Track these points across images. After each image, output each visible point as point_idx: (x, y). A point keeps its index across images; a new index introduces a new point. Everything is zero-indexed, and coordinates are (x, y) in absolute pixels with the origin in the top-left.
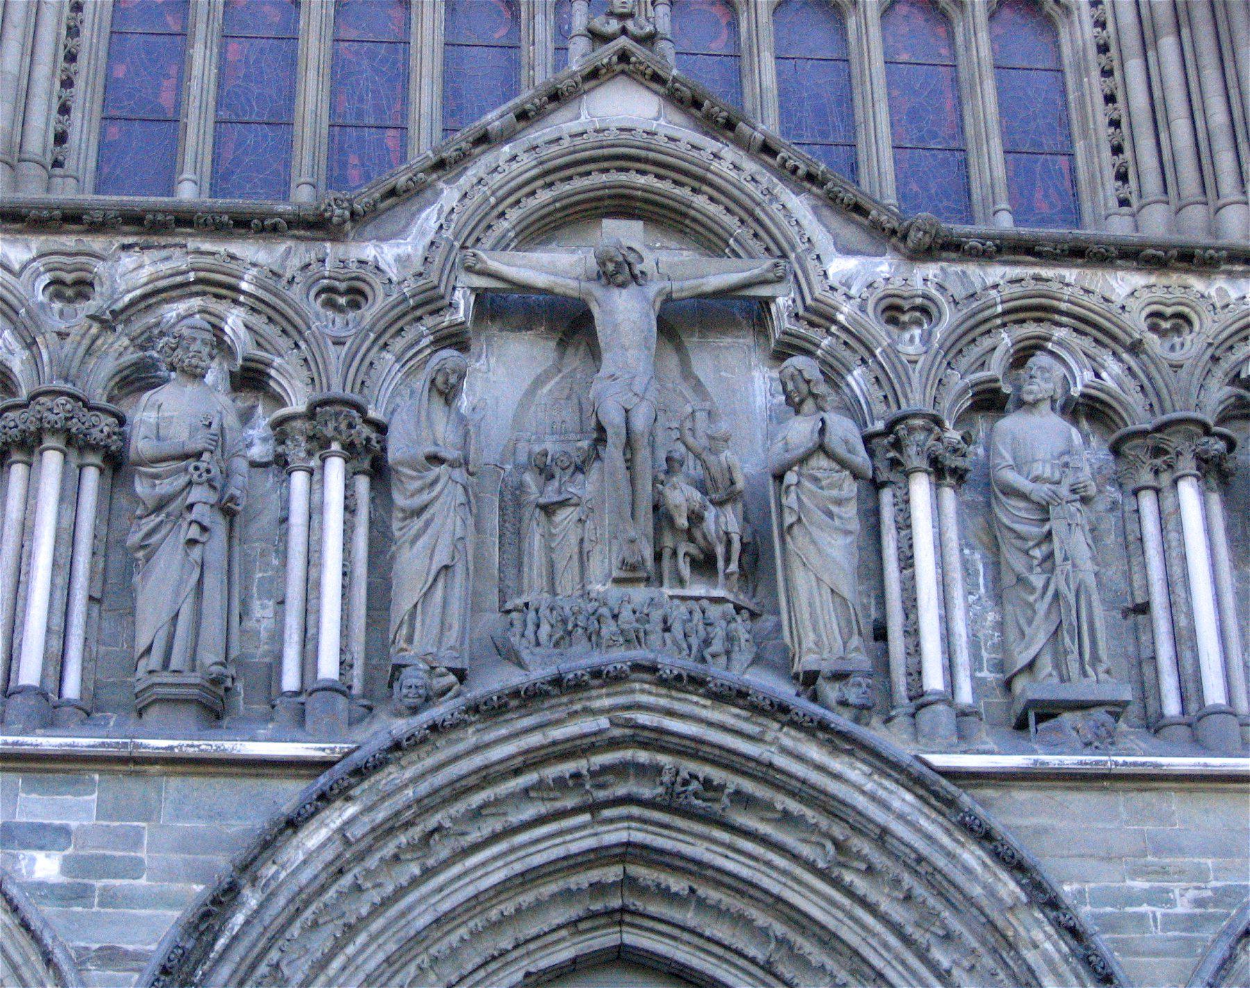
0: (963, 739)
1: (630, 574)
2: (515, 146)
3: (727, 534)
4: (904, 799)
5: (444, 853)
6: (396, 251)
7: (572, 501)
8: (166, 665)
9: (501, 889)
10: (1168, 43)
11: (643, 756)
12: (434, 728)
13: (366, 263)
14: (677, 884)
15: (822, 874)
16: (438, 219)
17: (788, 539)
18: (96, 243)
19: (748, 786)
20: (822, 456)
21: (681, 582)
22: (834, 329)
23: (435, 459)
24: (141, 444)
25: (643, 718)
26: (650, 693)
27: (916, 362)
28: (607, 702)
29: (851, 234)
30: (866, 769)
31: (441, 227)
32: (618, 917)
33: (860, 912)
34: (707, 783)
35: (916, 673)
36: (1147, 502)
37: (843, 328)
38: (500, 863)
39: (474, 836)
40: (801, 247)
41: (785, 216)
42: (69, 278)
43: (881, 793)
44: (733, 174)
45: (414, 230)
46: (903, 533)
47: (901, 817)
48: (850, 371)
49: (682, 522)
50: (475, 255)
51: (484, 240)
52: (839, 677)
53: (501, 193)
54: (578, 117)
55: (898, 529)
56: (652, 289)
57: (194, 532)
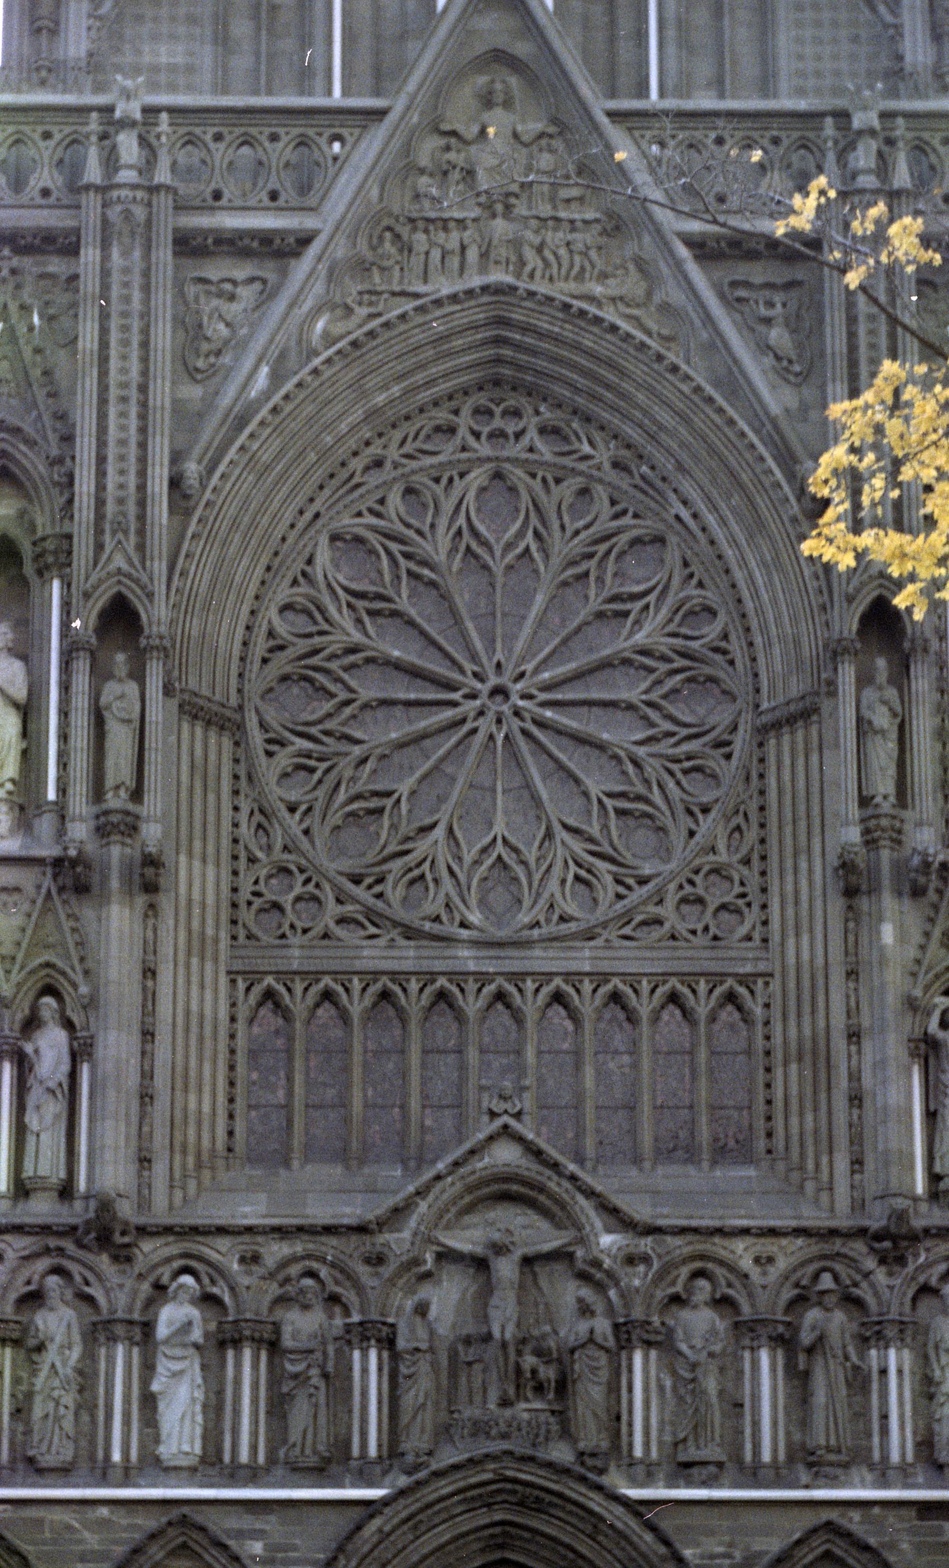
0: (649, 1480)
1: (505, 1403)
4: (619, 1510)
8: (303, 1451)
9: (448, 1543)
10: (794, 1067)
11: (509, 1486)
14: (526, 1535)
15: (589, 1536)
18: (260, 1239)
21: (527, 1400)
23: (417, 1350)
24: (287, 1342)
25: (509, 1473)
29: (612, 1221)
32: (501, 1547)
33: (605, 1553)
35: (631, 1445)
36: (747, 1355)
42: (249, 1255)
49: (528, 1375)
52: (593, 1455)
56: (518, 1253)
57: (312, 1390)
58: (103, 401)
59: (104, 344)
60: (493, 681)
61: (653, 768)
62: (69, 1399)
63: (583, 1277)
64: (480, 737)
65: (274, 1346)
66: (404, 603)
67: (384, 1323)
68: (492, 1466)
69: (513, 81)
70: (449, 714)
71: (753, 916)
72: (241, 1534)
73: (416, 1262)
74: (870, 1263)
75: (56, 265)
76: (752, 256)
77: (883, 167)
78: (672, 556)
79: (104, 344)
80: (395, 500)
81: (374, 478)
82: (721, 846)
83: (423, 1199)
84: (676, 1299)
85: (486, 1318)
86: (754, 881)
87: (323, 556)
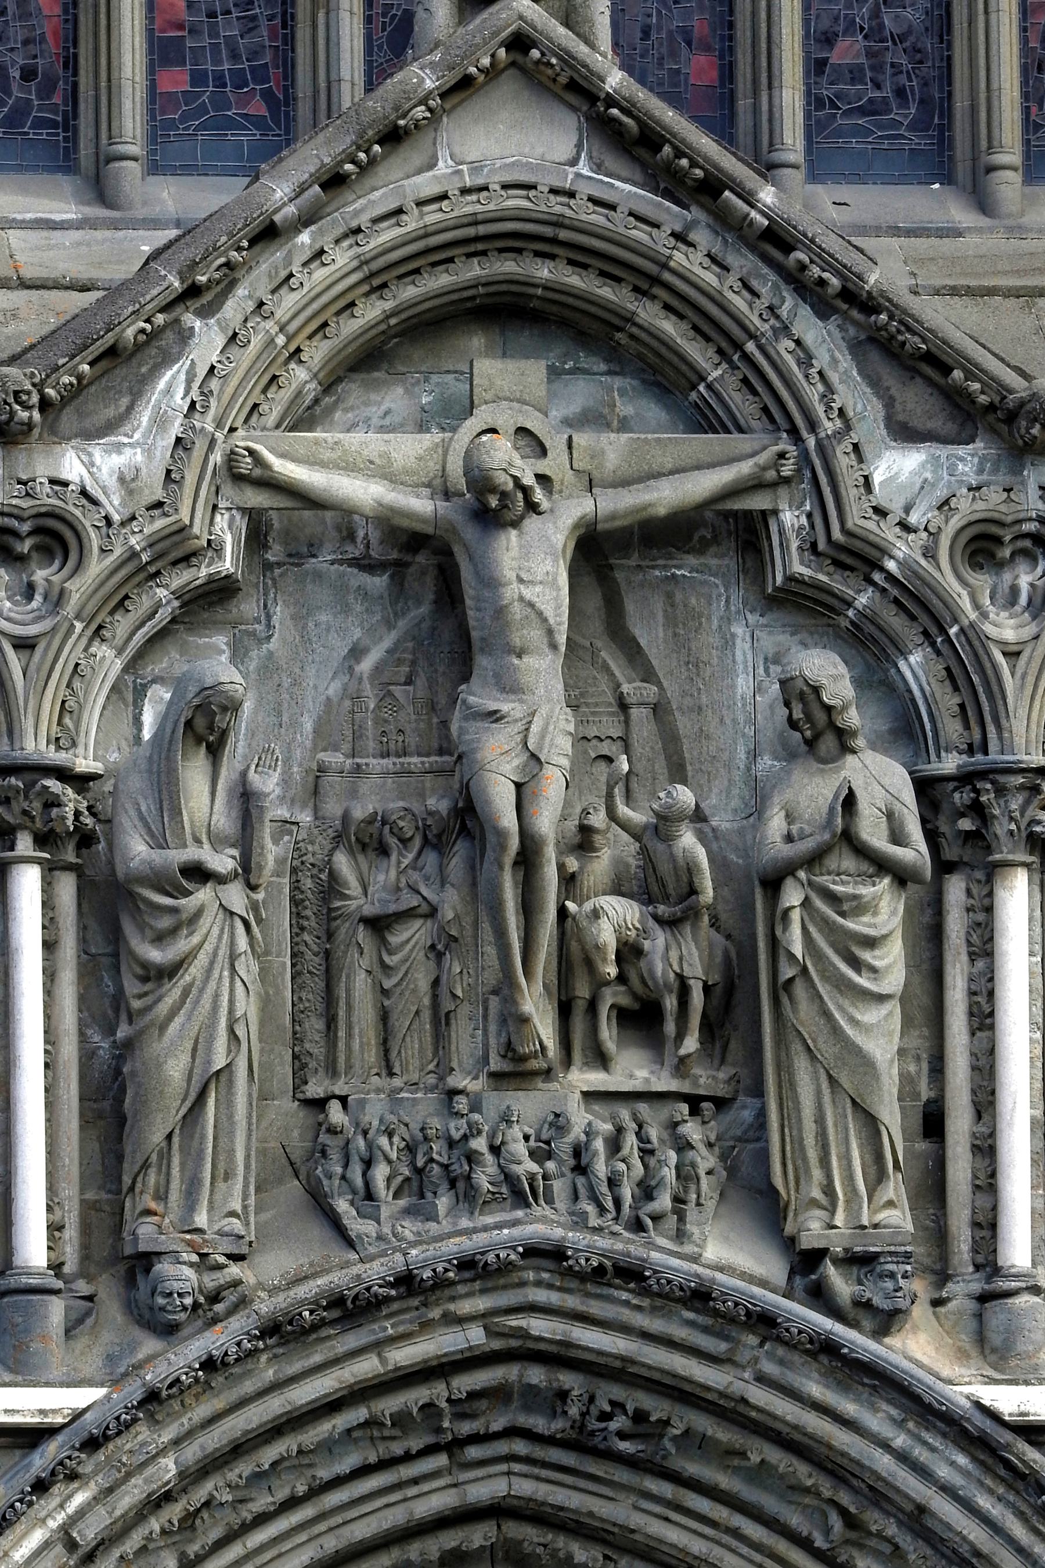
2: (321, 232)
3: (681, 978)
5: (215, 1534)
6: (117, 461)
7: (420, 911)
11: (536, 1375)
12: (209, 1364)
13: (65, 484)
16: (187, 392)
17: (785, 1000)
19: (704, 1424)
20: (846, 850)
21: (601, 1059)
22: (877, 577)
26: (550, 1286)
27: (1018, 654)
28: (481, 1304)
30: (894, 1412)
31: (193, 404)
34: (640, 1417)
37: (890, 577)
38: (303, 1537)
39: (263, 1502)
40: (829, 426)
41: (799, 363)
43: (920, 1453)
44: (709, 278)
45: (144, 417)
46: (980, 964)
47: (947, 1490)
48: (904, 654)
50: (251, 452)
51: (264, 408)
53: (292, 328)
54: (432, 165)
55: (973, 957)
67: (63, 774)
68: (481, 1304)
83: (204, 313)
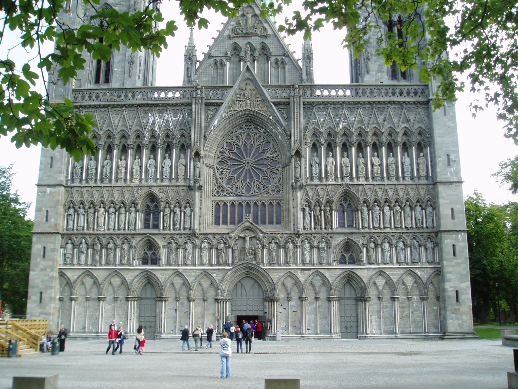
58: (195, 126)
59: (195, 118)
60: (247, 161)
61: (268, 173)
62: (190, 256)
63: (258, 240)
64: (245, 169)
65: (217, 249)
66: (235, 151)
69: (250, 82)
70: (241, 166)
71: (281, 192)
72: (212, 273)
73: (235, 238)
74: (295, 238)
75: (189, 108)
76: (281, 104)
77: (299, 93)
78: (271, 144)
79: (195, 118)
80: (235, 138)
81: (232, 135)
82: (277, 182)
84: (270, 243)
85: (244, 245)
86: (282, 187)
87: (225, 145)
